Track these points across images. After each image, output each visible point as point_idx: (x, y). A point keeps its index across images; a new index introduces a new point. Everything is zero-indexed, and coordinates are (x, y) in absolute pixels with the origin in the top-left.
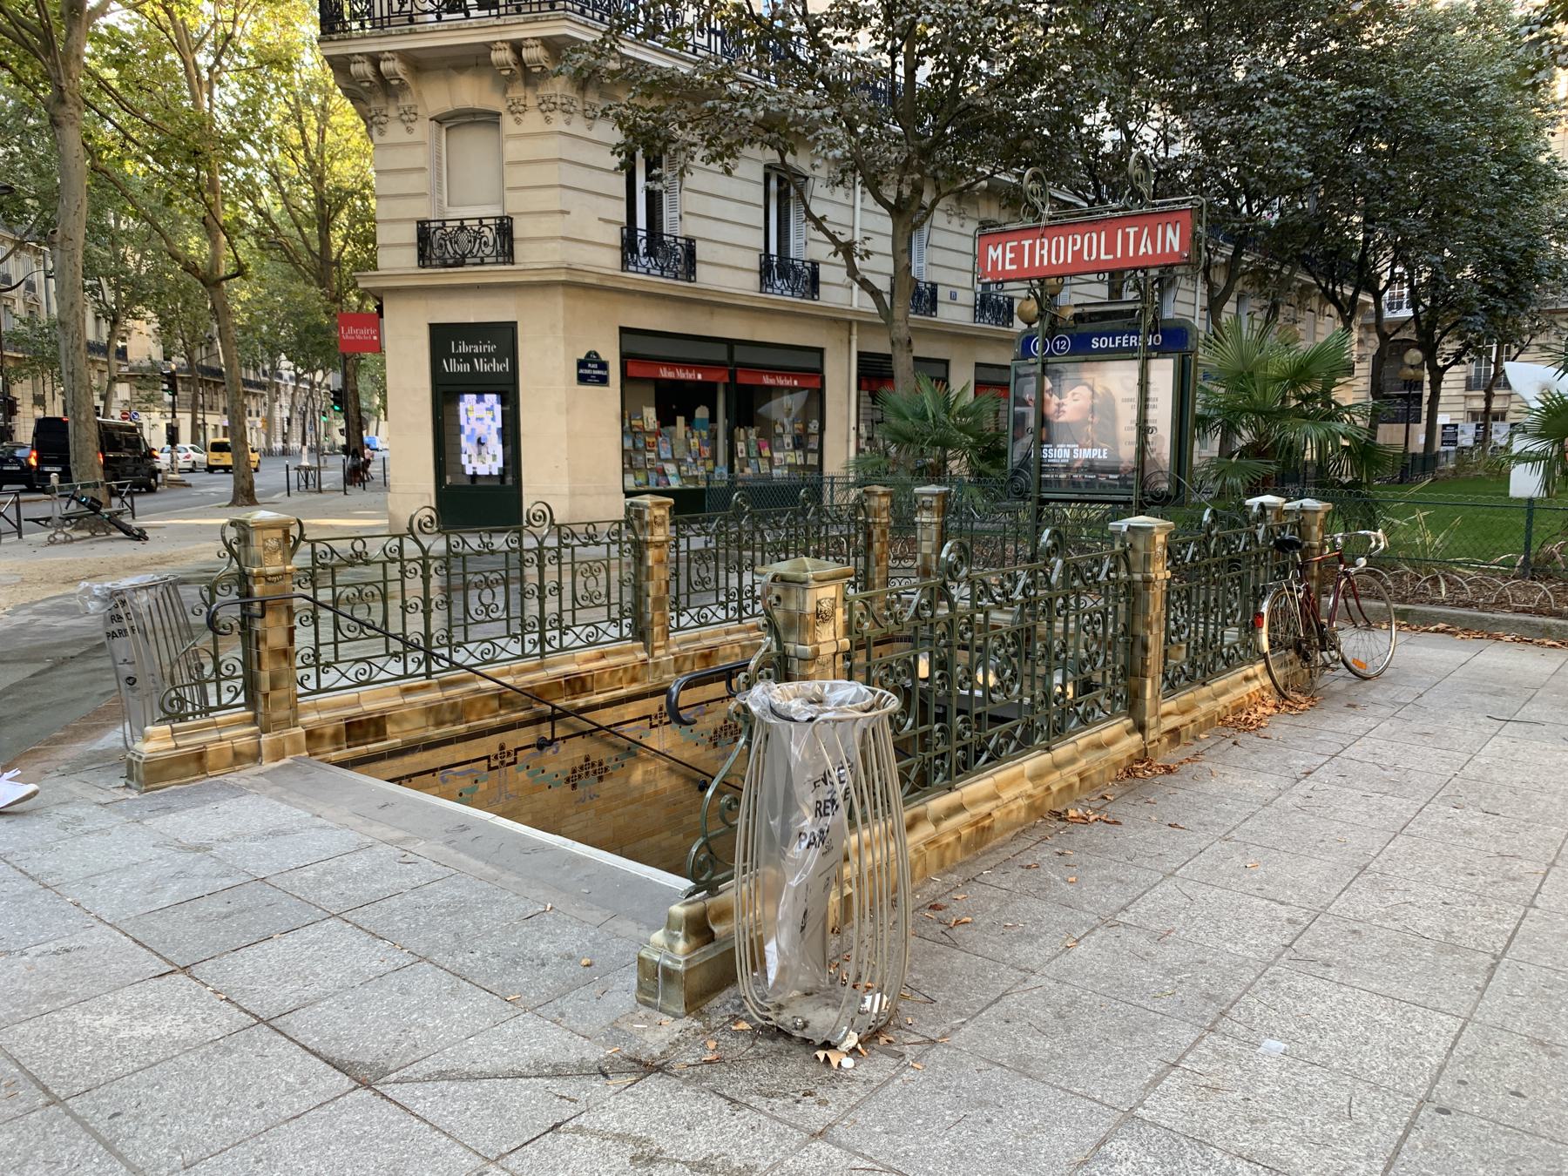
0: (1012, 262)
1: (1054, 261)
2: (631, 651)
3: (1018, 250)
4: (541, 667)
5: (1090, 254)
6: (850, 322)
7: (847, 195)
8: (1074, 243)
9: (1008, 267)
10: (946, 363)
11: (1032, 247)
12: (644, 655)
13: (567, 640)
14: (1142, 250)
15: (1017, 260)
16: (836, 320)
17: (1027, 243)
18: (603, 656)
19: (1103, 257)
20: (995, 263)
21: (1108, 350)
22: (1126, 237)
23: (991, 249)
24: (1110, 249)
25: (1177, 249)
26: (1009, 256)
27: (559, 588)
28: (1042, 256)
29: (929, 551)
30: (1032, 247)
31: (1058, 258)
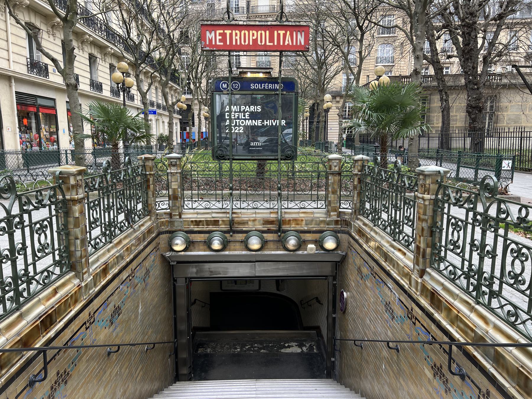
0: (220, 41)
1: (243, 43)
2: (69, 280)
4: (21, 317)
5: (261, 42)
8: (253, 35)
9: (218, 43)
10: (54, 100)
11: (231, 35)
12: (76, 281)
13: (33, 287)
14: (287, 43)
15: (224, 40)
17: (228, 32)
18: (55, 292)
19: (268, 44)
20: (211, 41)
21: (258, 90)
22: (279, 35)
23: (208, 33)
24: (271, 40)
25: (303, 44)
26: (218, 38)
27: (24, 248)
28: (236, 40)
29: (176, 187)
30: (231, 35)
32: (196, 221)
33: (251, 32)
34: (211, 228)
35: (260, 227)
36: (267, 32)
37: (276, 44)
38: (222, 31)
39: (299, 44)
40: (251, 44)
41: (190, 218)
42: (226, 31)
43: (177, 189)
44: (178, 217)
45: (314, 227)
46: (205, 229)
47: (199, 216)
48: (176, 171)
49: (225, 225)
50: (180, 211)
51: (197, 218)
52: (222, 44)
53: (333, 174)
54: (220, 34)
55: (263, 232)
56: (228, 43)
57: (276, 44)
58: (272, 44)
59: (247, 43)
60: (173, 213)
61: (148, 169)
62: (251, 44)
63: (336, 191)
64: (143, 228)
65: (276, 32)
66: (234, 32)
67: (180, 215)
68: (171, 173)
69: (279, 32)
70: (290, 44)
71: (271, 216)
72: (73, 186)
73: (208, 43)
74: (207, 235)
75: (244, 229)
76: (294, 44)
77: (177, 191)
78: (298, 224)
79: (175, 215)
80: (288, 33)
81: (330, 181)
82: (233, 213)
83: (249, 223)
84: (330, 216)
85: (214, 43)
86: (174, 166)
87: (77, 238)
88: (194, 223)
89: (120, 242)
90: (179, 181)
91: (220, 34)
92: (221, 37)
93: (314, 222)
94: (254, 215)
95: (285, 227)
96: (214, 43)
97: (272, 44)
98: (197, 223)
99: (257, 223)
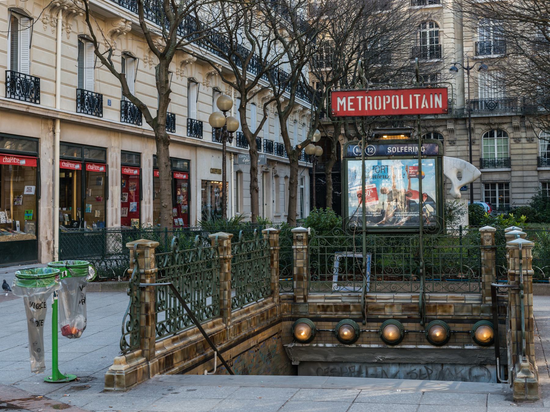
0: (352, 107)
3: (355, 101)
5: (395, 106)
6: (54, 120)
7: (53, 31)
9: (349, 109)
11: (363, 100)
14: (423, 106)
15: (355, 106)
16: (46, 118)
17: (360, 98)
19: (402, 108)
20: (341, 107)
22: (414, 99)
23: (339, 99)
24: (406, 104)
25: (441, 106)
26: (350, 104)
28: (369, 105)
29: (301, 265)
30: (363, 100)
31: (378, 107)
32: (323, 306)
33: (384, 97)
34: (340, 314)
35: (397, 312)
36: (402, 96)
37: (411, 107)
38: (353, 97)
39: (436, 107)
40: (384, 108)
41: (316, 303)
42: (357, 97)
43: (303, 267)
44: (303, 301)
45: (464, 314)
46: (333, 316)
47: (326, 301)
48: (302, 247)
49: (357, 311)
50: (305, 294)
51: (324, 302)
52: (353, 110)
53: (485, 249)
54: (352, 100)
55: (402, 321)
56: (360, 109)
57: (411, 107)
58: (407, 108)
59: (380, 108)
60: (298, 297)
61: (272, 243)
62: (384, 108)
63: (491, 271)
64: (267, 307)
65: (411, 96)
66: (366, 98)
67: (305, 299)
68: (297, 249)
69: (415, 95)
70: (427, 107)
71: (413, 301)
72: (225, 248)
73: (338, 110)
74: (335, 324)
75: (379, 317)
76: (432, 107)
77: (302, 270)
78: (445, 311)
79: (299, 299)
80: (424, 96)
81: (482, 258)
82: (366, 297)
83: (386, 309)
84: (485, 301)
85: (345, 110)
86: (300, 241)
87: (225, 290)
88: (321, 309)
89: (248, 311)
90: (305, 258)
91: (352, 100)
92: (352, 104)
93: (465, 309)
94: (392, 301)
95: (430, 314)
96: (345, 110)
97: (407, 108)
98: (325, 308)
99: (395, 308)
